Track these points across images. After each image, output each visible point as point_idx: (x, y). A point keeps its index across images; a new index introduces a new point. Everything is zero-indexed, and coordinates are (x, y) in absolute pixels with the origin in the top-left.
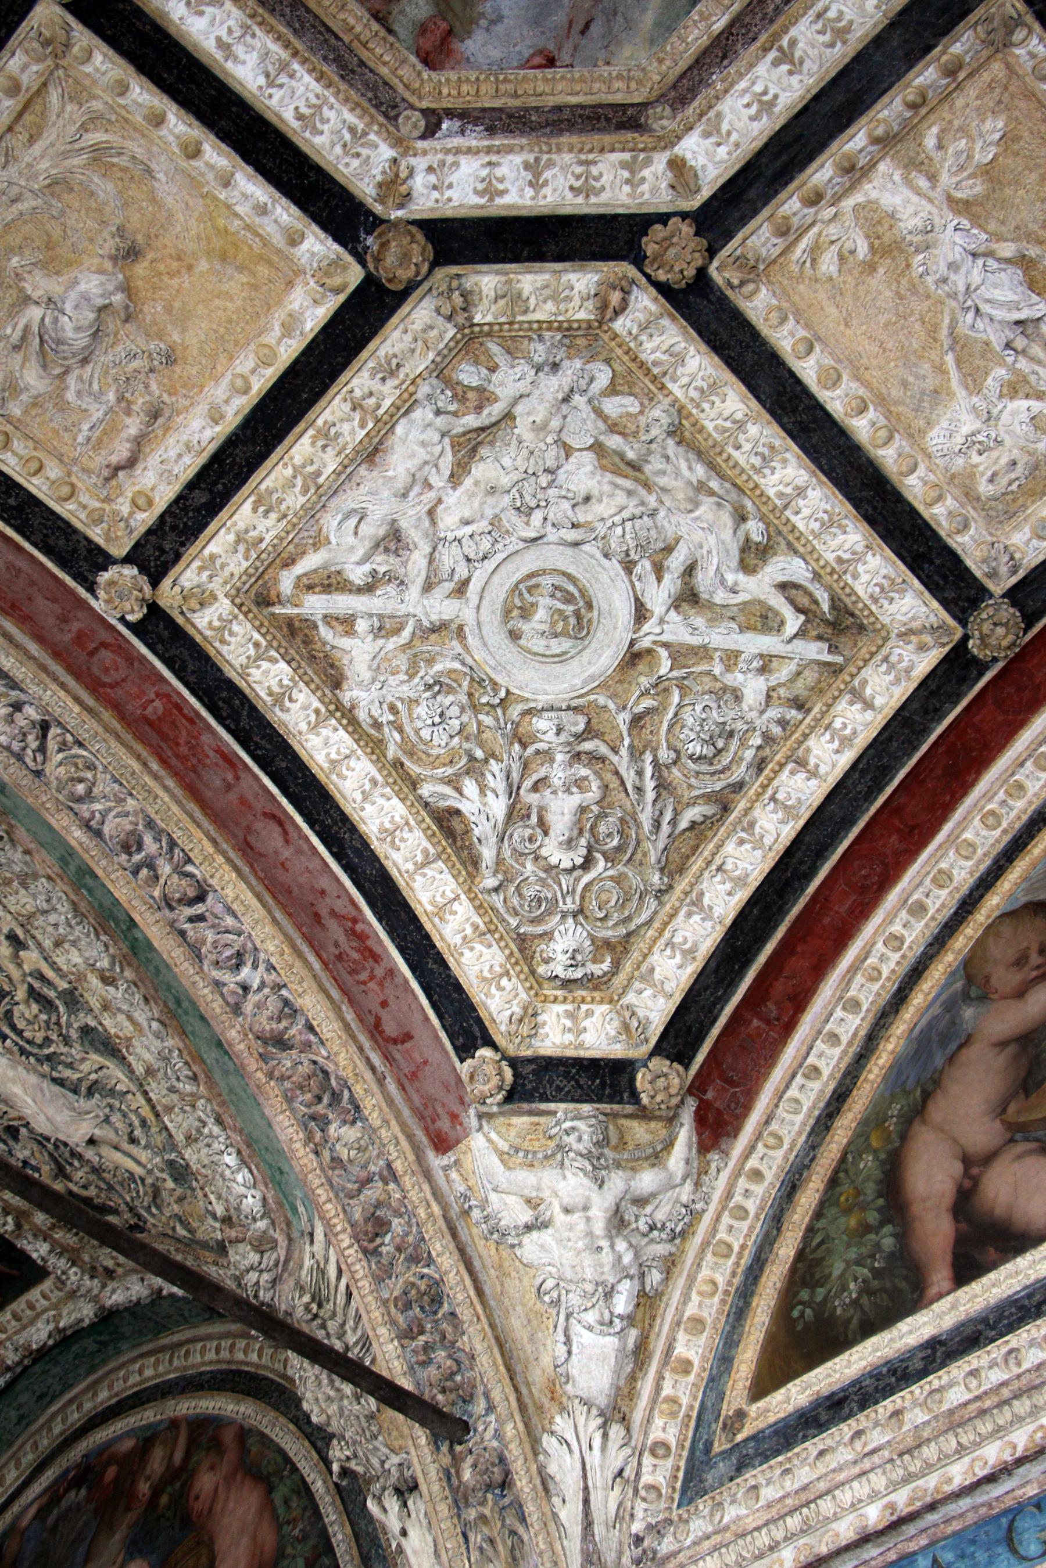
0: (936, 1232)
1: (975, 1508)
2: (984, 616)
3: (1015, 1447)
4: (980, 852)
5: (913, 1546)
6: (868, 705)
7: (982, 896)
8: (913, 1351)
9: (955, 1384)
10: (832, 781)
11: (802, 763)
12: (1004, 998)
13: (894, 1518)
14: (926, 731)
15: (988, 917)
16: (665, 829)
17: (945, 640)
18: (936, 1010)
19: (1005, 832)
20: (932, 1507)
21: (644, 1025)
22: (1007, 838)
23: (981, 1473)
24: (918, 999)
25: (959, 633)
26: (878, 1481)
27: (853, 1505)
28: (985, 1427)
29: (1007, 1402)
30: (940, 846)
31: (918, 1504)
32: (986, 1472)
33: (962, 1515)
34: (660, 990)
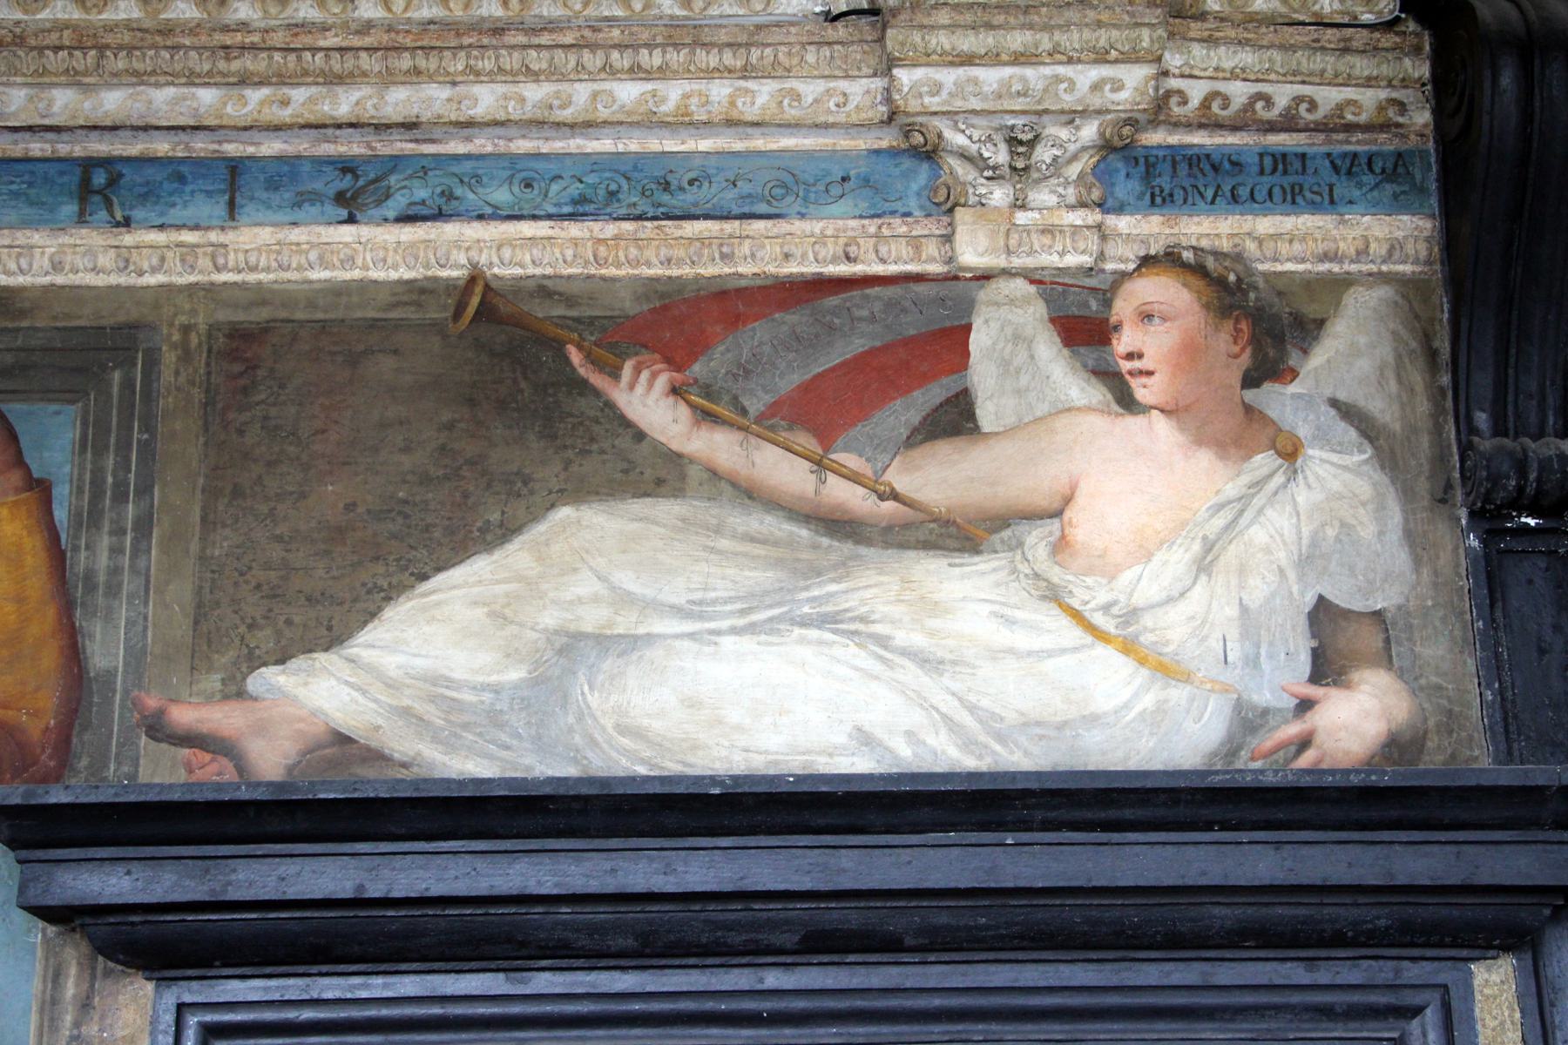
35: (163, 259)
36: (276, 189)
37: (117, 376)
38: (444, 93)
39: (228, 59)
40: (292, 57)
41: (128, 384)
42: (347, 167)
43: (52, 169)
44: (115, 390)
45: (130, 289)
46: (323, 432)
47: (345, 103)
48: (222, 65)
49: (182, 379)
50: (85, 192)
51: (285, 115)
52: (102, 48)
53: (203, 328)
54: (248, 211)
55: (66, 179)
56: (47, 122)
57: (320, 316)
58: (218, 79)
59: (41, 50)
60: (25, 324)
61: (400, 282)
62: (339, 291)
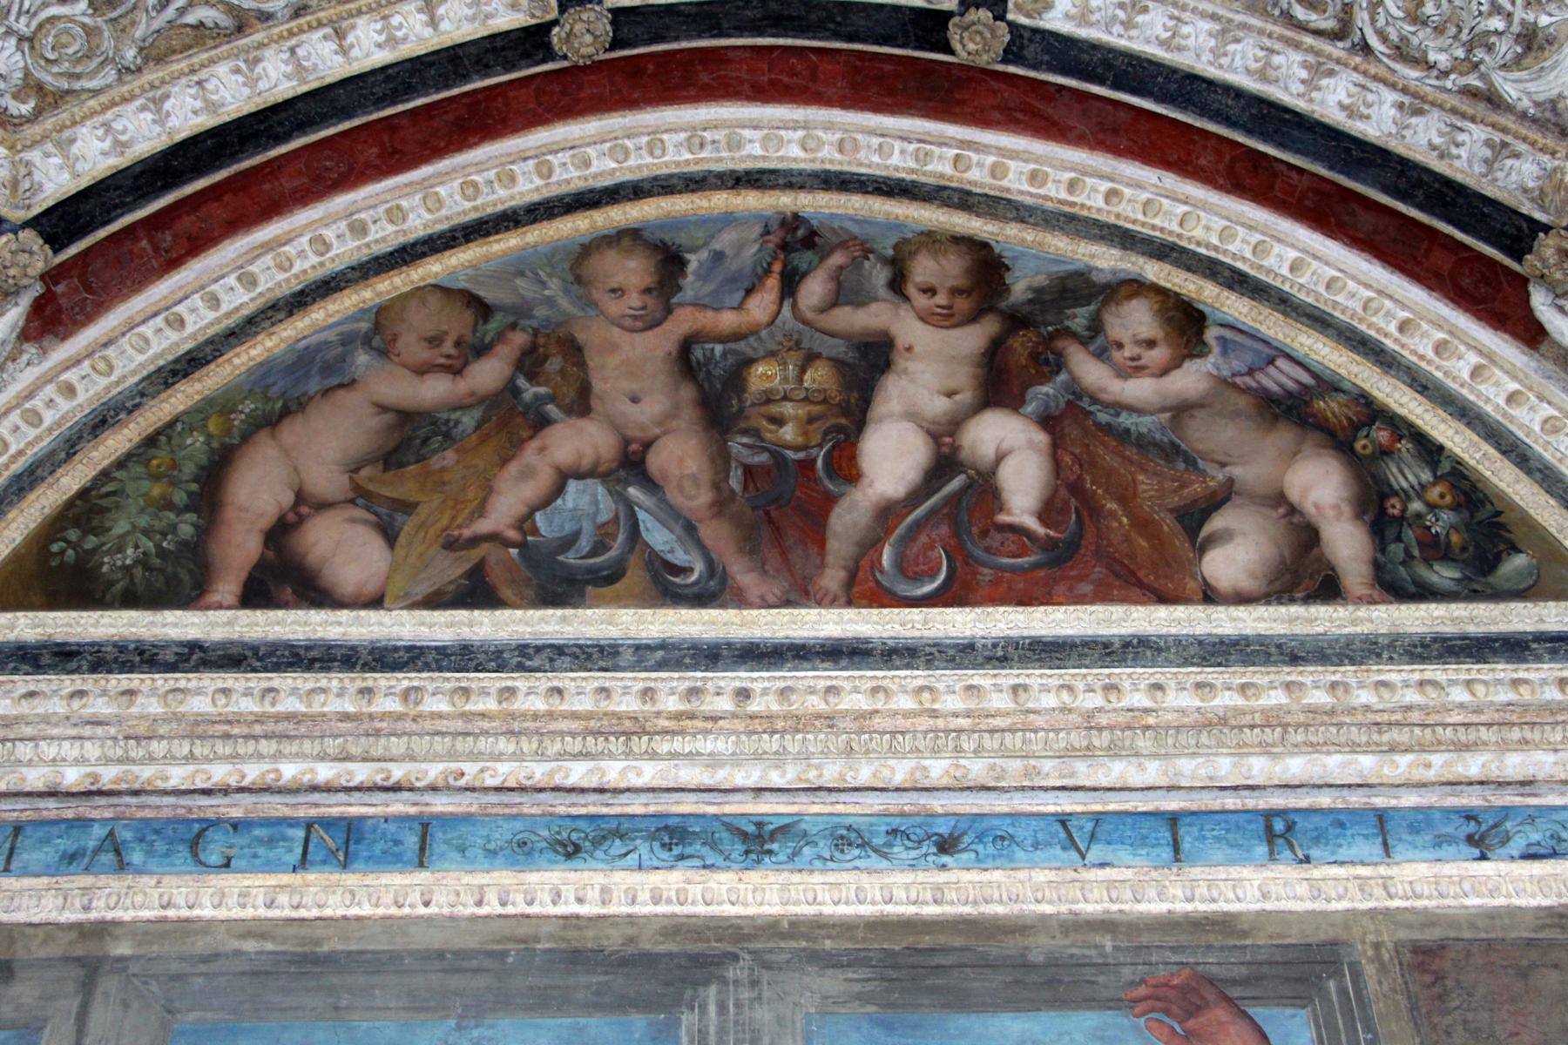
0: (241, 546)
1: (175, 807)
2: (585, 17)
3: (243, 777)
4: (444, 212)
5: (95, 814)
6: (433, 23)
7: (424, 255)
8: (167, 645)
9: (203, 693)
10: (356, 68)
11: (340, 35)
12: (403, 365)
13: (94, 788)
14: (466, 78)
15: (423, 279)
16: (170, 12)
17: (538, 13)
18: (331, 336)
19: (476, 208)
20: (136, 793)
21: (36, 189)
22: (475, 216)
23: (200, 785)
24: (321, 314)
25: (553, 15)
26: (92, 750)
27: (54, 760)
28: (224, 748)
29: (256, 738)
30: (411, 184)
31: (124, 786)
32: (205, 786)
33: (158, 807)
34: (70, 164)
35: (1346, 889)
36: (1418, 832)
37: (1332, 984)
38: (1549, 758)
39: (1380, 732)
40: (1428, 731)
41: (1343, 992)
42: (1470, 816)
43: (1241, 818)
44: (1335, 998)
45: (1323, 913)
46: (1517, 1034)
47: (1474, 765)
48: (1375, 737)
49: (1385, 988)
50: (1270, 836)
51: (1430, 775)
52: (1285, 726)
53: (1390, 945)
54: (1399, 851)
55: (1253, 826)
56: (1250, 782)
57: (1483, 935)
58: (1374, 748)
59: (1240, 728)
60: (1249, 942)
61: (1539, 908)
62: (1492, 915)
